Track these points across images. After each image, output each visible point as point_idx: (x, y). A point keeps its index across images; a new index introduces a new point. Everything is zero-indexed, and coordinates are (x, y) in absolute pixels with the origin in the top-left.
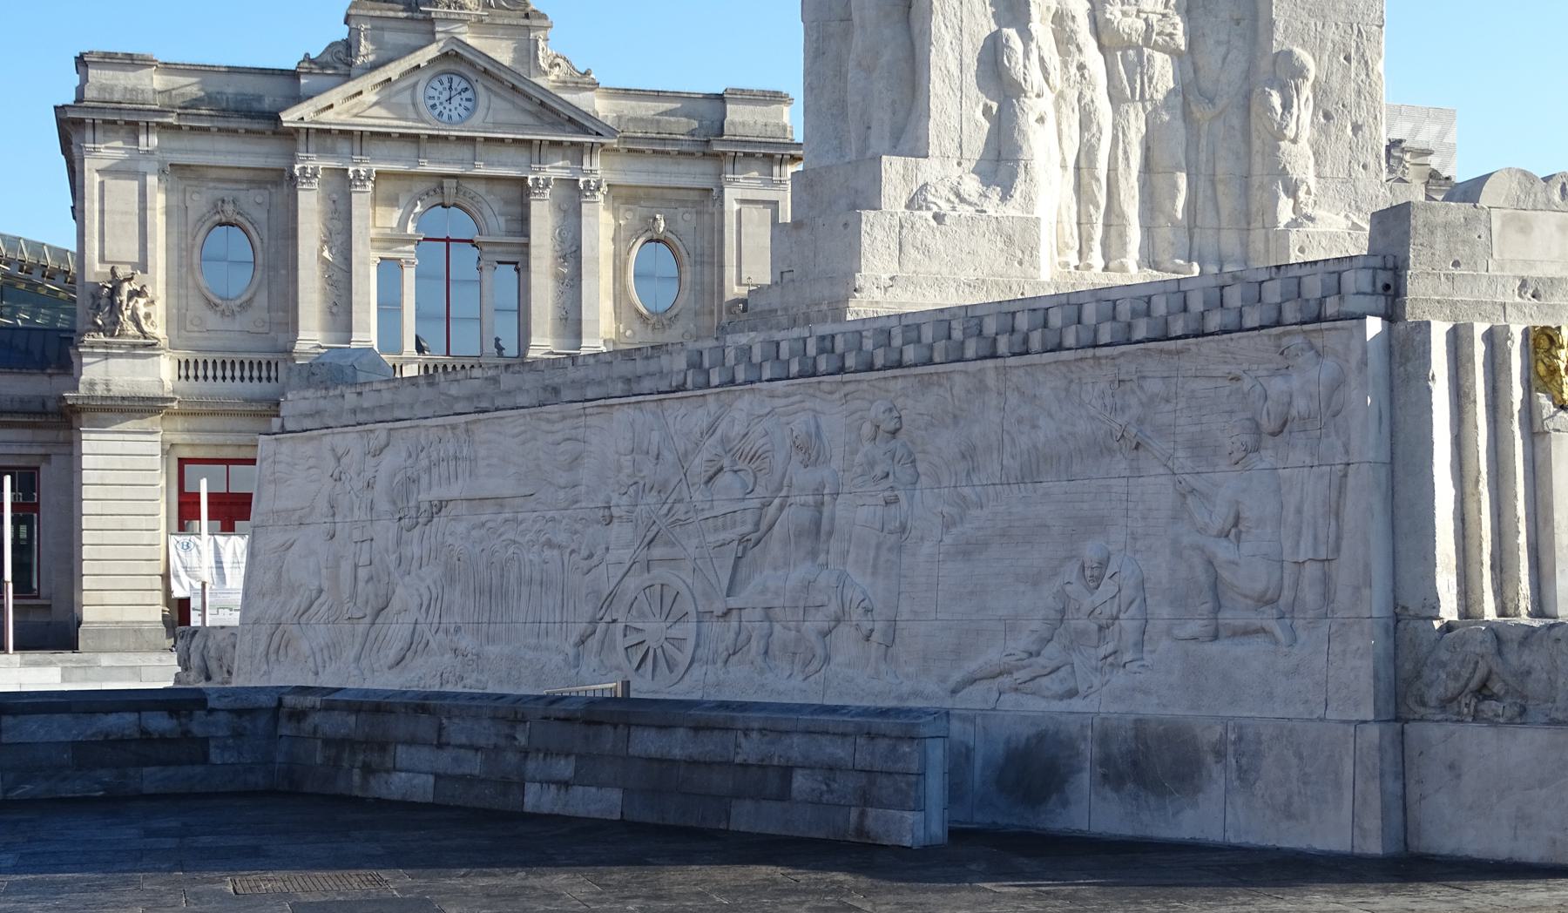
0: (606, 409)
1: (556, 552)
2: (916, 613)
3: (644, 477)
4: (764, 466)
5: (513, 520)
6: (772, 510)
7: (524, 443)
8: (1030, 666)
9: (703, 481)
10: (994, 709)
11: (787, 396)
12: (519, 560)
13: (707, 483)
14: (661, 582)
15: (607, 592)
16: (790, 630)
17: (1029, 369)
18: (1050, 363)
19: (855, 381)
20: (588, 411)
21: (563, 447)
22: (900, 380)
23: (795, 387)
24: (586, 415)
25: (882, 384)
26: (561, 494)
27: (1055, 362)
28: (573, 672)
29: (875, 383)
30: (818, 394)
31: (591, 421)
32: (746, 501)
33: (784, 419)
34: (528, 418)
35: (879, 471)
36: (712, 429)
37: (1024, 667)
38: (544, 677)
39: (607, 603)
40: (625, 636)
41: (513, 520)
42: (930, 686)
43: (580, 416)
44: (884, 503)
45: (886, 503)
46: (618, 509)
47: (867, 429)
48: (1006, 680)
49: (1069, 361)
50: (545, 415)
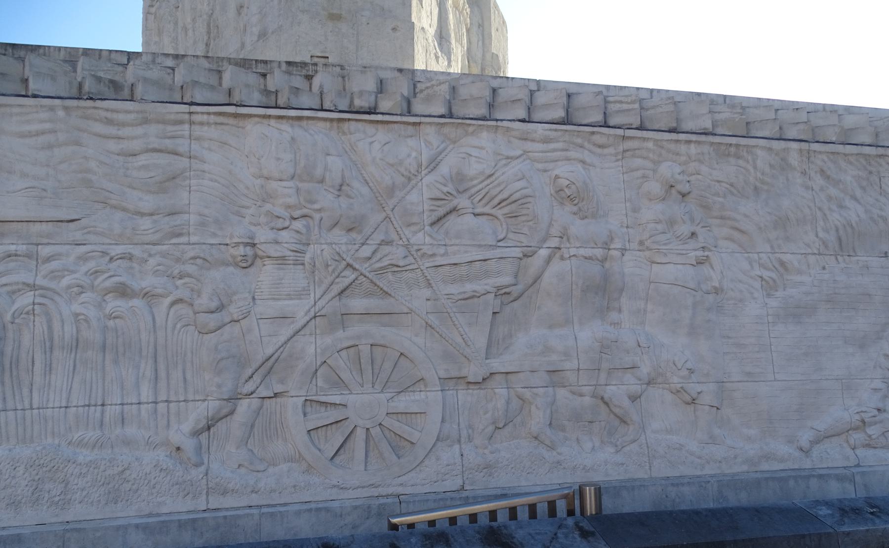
0: (231, 121)
1: (137, 302)
2: (749, 374)
3: (319, 210)
4: (524, 212)
5: (29, 256)
6: (536, 262)
7: (50, 147)
8: (881, 422)
9: (427, 221)
10: (858, 466)
11: (546, 140)
12: (47, 314)
13: (432, 224)
14: (371, 342)
15: (260, 358)
16: (581, 395)
17: (832, 157)
18: (852, 154)
19: (640, 138)
20: (197, 118)
21: (142, 160)
22: (692, 146)
23: (560, 133)
24: (191, 123)
25: (672, 146)
26: (146, 223)
27: (857, 154)
28: (196, 474)
29: (664, 143)
30: (586, 144)
31: (197, 131)
32: (499, 250)
33: (540, 166)
34: (61, 113)
35: (684, 229)
36: (434, 164)
37: (875, 423)
38: (127, 486)
39: (263, 370)
40: (305, 415)
41: (29, 256)
42: (782, 449)
43: (181, 122)
44: (694, 263)
45: (697, 263)
46: (278, 247)
47: (655, 188)
48: (857, 437)
49: (869, 155)
50: (103, 114)
